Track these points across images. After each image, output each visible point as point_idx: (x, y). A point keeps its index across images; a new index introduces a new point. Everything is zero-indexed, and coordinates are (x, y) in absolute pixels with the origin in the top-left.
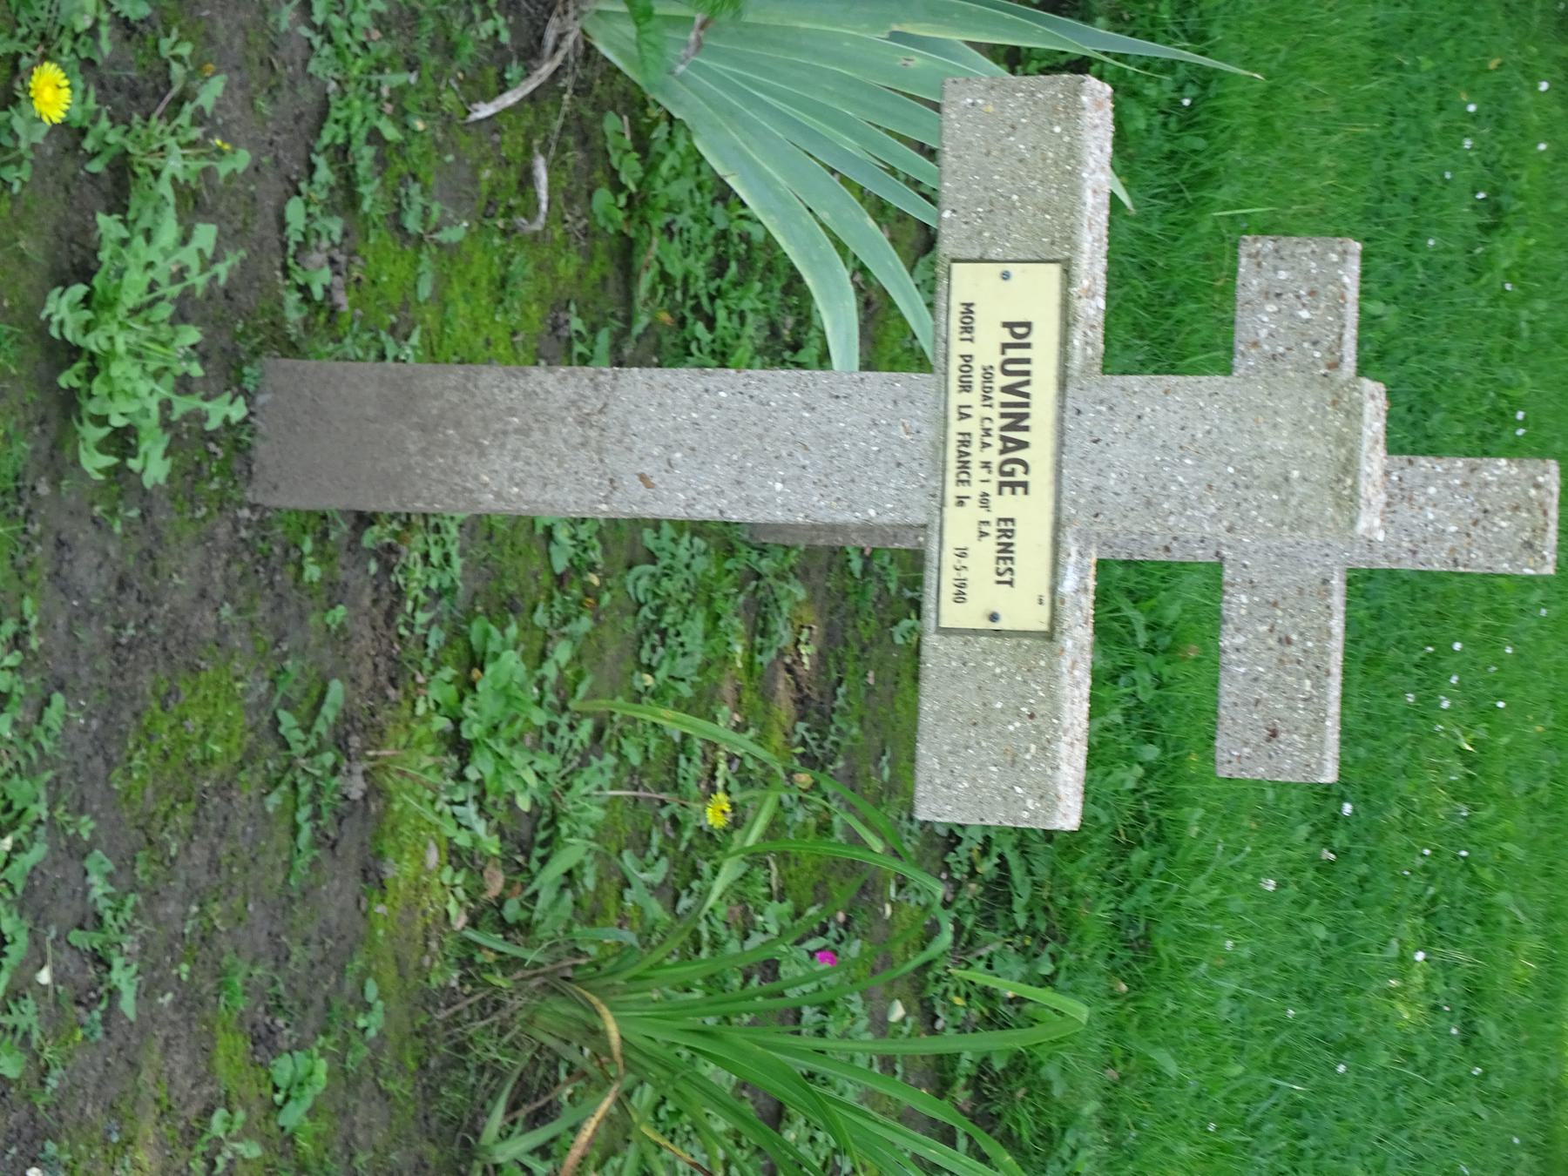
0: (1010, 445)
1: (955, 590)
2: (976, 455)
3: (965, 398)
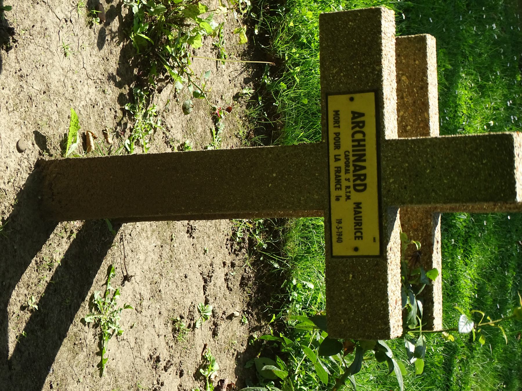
0: (357, 168)
1: (337, 237)
2: (343, 176)
3: (337, 152)
